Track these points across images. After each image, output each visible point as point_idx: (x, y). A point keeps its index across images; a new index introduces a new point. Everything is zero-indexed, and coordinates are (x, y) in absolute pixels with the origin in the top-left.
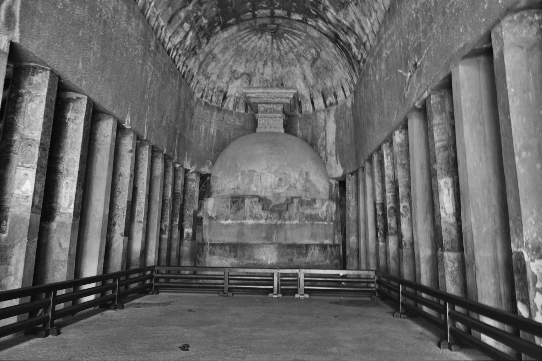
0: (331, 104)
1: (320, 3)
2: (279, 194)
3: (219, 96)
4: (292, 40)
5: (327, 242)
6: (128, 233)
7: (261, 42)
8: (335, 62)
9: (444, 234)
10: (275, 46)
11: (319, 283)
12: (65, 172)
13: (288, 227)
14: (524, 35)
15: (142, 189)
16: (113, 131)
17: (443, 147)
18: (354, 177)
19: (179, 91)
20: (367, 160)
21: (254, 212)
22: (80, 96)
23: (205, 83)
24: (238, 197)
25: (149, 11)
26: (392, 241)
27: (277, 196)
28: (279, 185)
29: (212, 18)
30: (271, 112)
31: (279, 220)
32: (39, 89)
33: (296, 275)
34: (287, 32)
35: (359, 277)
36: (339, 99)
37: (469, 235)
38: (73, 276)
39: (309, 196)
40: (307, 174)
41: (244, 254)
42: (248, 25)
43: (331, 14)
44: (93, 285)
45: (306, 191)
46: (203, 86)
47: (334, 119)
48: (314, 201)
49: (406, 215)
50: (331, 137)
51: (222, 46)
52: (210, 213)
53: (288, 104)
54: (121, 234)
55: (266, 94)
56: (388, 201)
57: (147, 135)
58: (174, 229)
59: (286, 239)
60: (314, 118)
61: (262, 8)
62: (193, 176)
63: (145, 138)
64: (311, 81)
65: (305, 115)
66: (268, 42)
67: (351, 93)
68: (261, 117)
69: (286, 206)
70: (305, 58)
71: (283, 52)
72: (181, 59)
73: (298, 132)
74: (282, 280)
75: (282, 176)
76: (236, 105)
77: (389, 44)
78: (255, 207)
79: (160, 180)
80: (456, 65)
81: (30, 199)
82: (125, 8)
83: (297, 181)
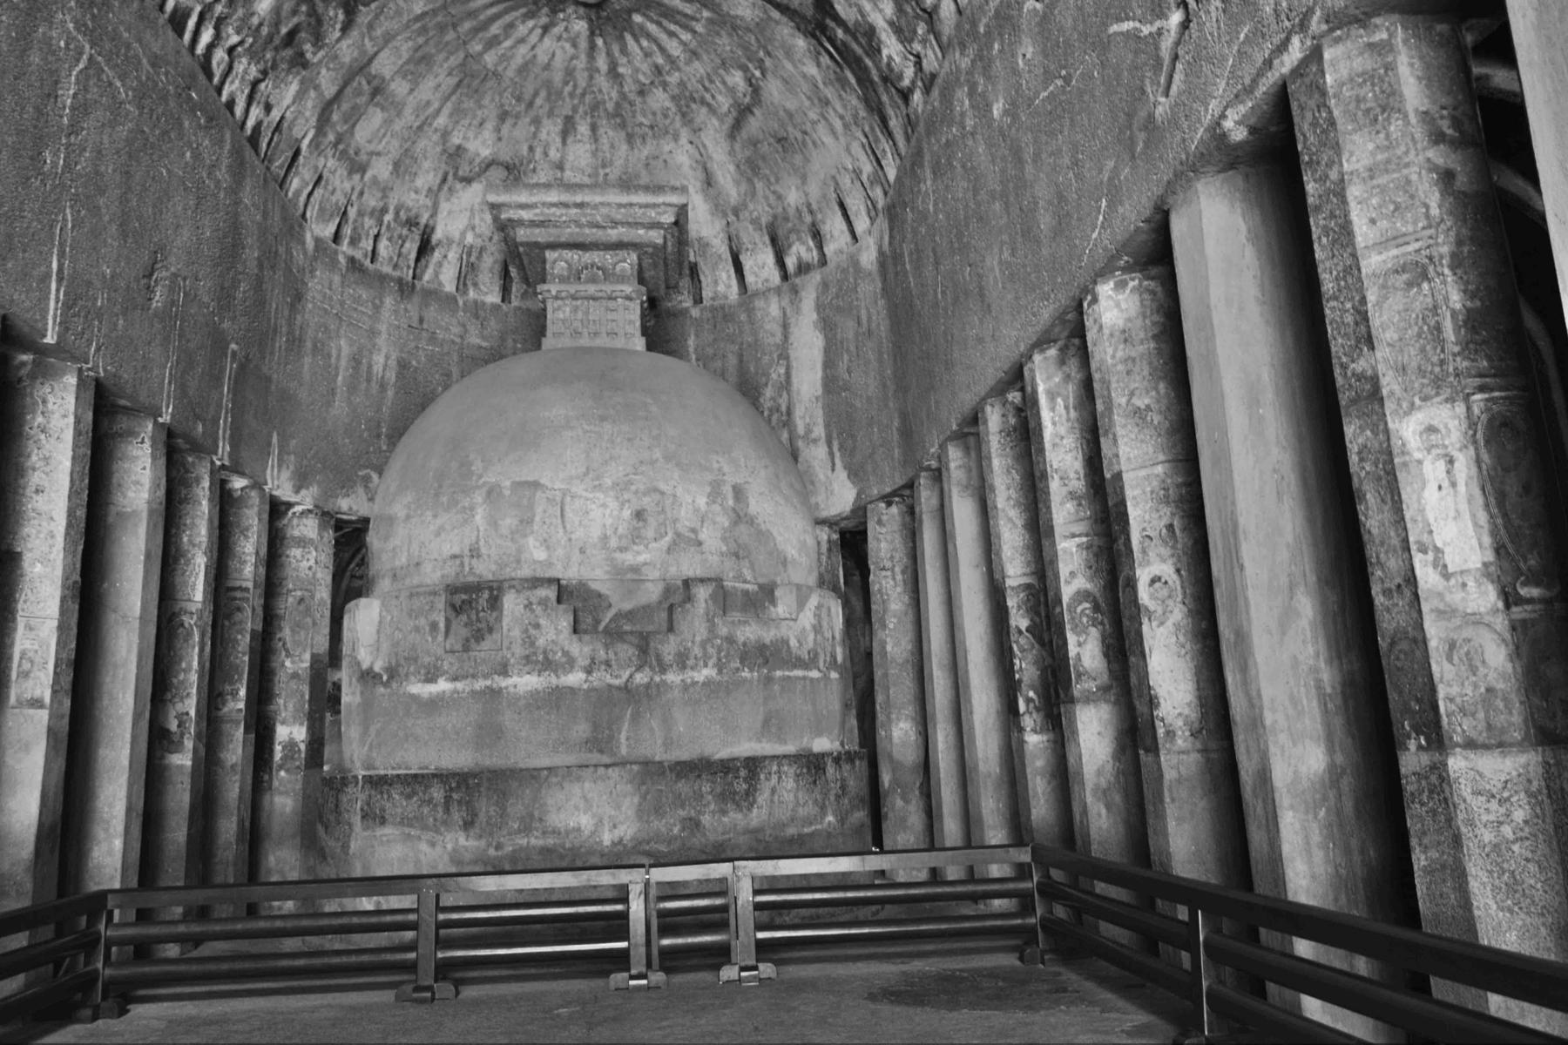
0: (803, 268)
2: (635, 569)
4: (663, 37)
10: (602, 63)
15: (45, 561)
18: (894, 510)
20: (950, 439)
21: (541, 642)
23: (347, 186)
24: (477, 588)
27: (630, 577)
28: (636, 537)
30: (593, 280)
31: (639, 668)
33: (721, 888)
36: (829, 249)
39: (748, 575)
40: (738, 492)
41: (503, 814)
45: (737, 555)
47: (815, 316)
48: (768, 592)
50: (808, 380)
51: (405, 47)
52: (365, 657)
53: (655, 246)
55: (574, 211)
57: (65, 326)
59: (668, 744)
60: (743, 317)
63: (50, 339)
64: (732, 190)
65: (713, 309)
66: (575, 45)
68: (556, 298)
69: (664, 615)
70: (709, 105)
71: (629, 87)
72: (240, 67)
74: (663, 914)
75: (647, 502)
76: (465, 278)
78: (542, 622)
79: (142, 530)
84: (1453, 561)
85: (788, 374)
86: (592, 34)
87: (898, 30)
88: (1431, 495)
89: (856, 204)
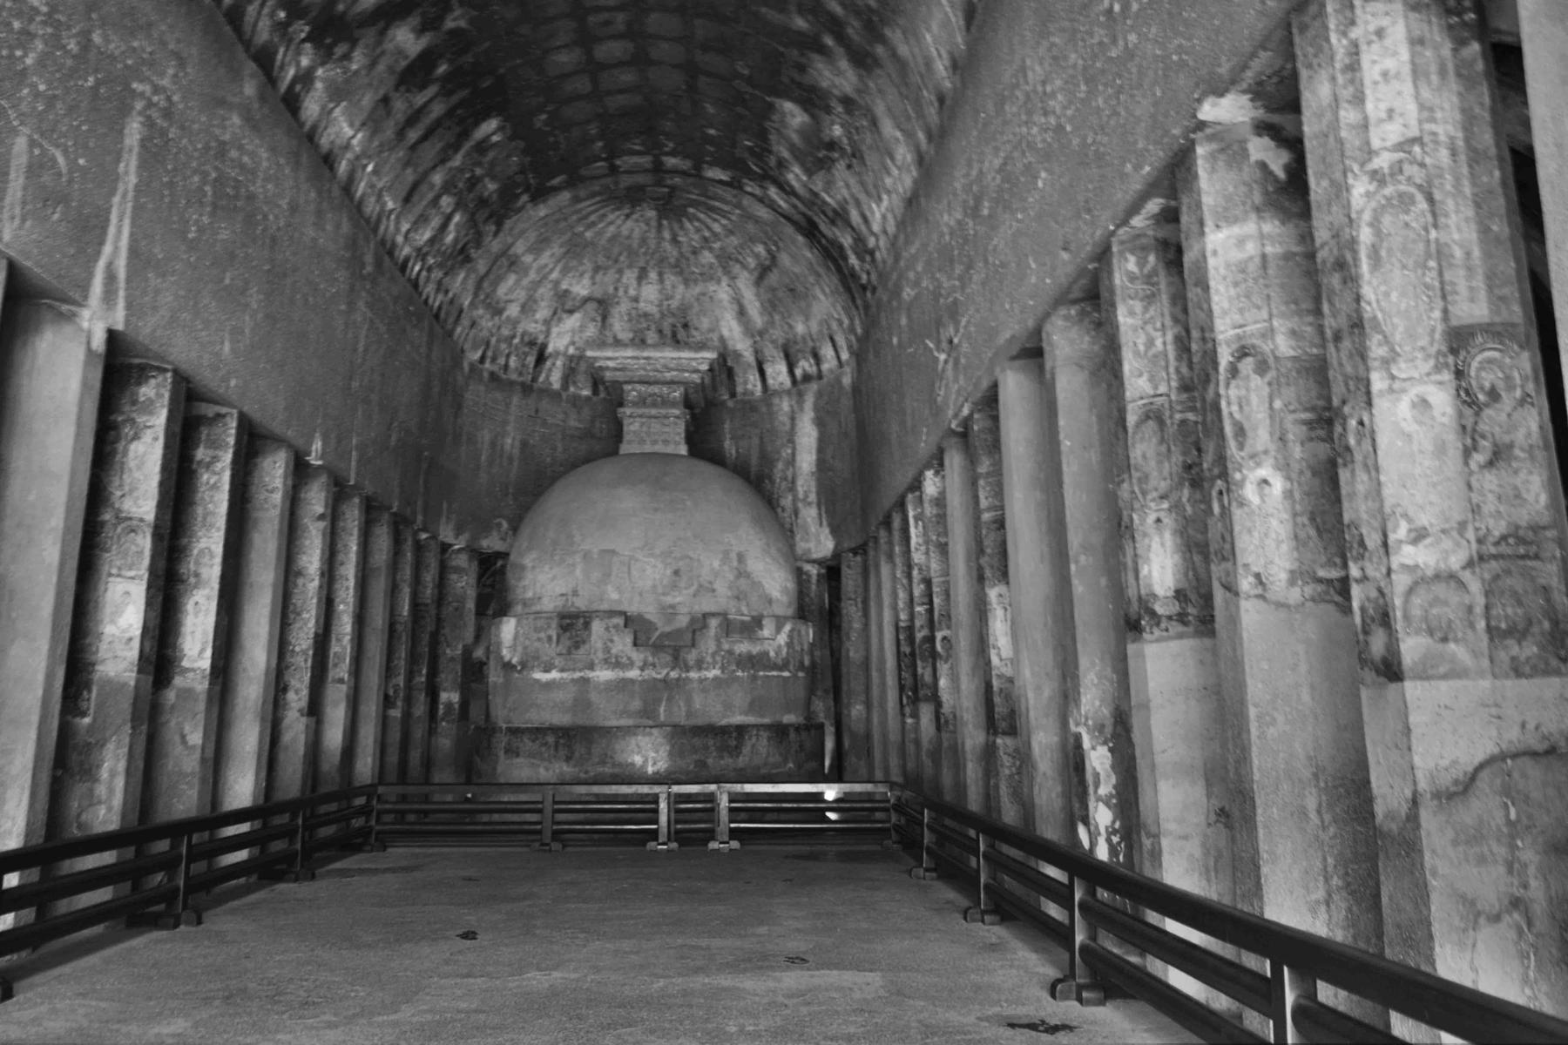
0: (807, 378)
1: (770, 152)
2: (672, 607)
3: (526, 354)
4: (708, 221)
5: (789, 718)
6: (315, 709)
7: (631, 226)
8: (811, 279)
10: (667, 235)
11: (769, 816)
12: (192, 580)
13: (695, 685)
14: (1085, 346)
15: (346, 604)
16: (285, 477)
18: (859, 558)
19: (428, 356)
21: (614, 651)
22: (224, 410)
24: (576, 616)
25: (363, 184)
26: (926, 712)
27: (670, 612)
29: (509, 178)
30: (654, 405)
32: (151, 413)
33: (710, 798)
34: (694, 204)
35: (869, 797)
36: (825, 367)
38: (208, 807)
39: (745, 610)
40: (741, 558)
41: (589, 753)
42: (597, 188)
43: (795, 176)
44: (244, 828)
45: (738, 598)
46: (485, 333)
48: (758, 622)
50: (807, 460)
51: (532, 236)
52: (506, 653)
54: (300, 710)
56: (918, 623)
57: (357, 474)
58: (415, 693)
59: (689, 714)
62: (462, 560)
64: (758, 320)
65: (744, 402)
73: (727, 444)
74: (678, 811)
76: (567, 378)
80: (1003, 370)
81: (136, 644)
82: (313, 195)
83: (716, 574)
84: (1004, 655)
85: (794, 454)
86: (660, 218)
87: (856, 254)
89: (841, 340)
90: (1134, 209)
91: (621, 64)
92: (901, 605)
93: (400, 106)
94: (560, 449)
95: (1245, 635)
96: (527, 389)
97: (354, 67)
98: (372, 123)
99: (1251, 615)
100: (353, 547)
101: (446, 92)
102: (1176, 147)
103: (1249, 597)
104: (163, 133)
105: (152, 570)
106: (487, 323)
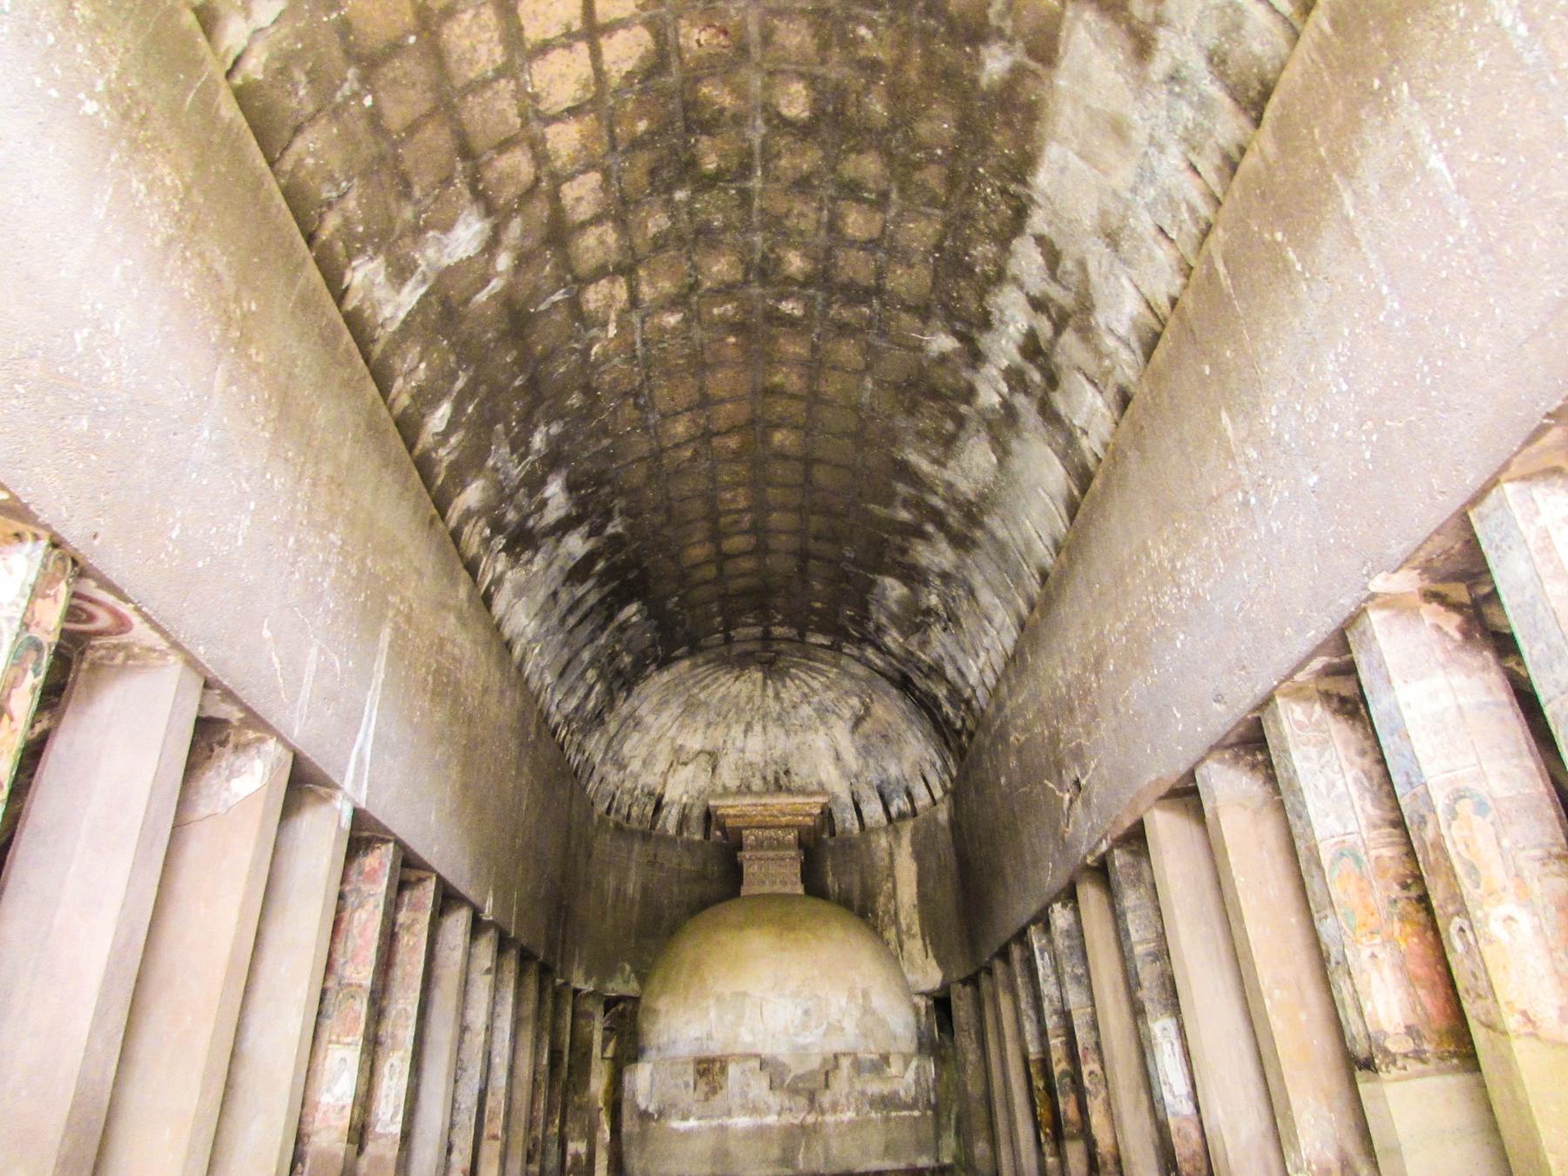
0: (902, 816)
2: (804, 1047)
4: (809, 680)
7: (743, 686)
8: (904, 726)
9: (1175, 1140)
10: (770, 692)
12: (389, 1041)
17: (1148, 954)
18: (968, 989)
21: (751, 1096)
22: (422, 874)
24: (712, 1061)
26: (1075, 1153)
27: (802, 1052)
30: (771, 847)
32: (374, 882)
34: (797, 665)
36: (919, 804)
37: (1218, 1144)
40: (865, 995)
42: (713, 656)
43: (893, 639)
45: (865, 1036)
46: (612, 788)
48: (885, 1059)
49: (1098, 1092)
51: (655, 699)
52: (642, 1103)
61: (746, 625)
66: (754, 684)
67: (946, 792)
73: (830, 880)
75: (810, 1004)
76: (683, 822)
77: (1020, 722)
82: (498, 676)
85: (895, 888)
86: (765, 678)
88: (1166, 1058)
90: (1301, 665)
91: (742, 554)
92: (1028, 1037)
93: (564, 598)
94: (676, 890)
95: (1524, 1076)
96: (646, 836)
97: (535, 569)
98: (544, 613)
99: (1524, 1054)
100: (510, 999)
101: (601, 584)
102: (1346, 614)
103: (1518, 1036)
104: (404, 634)
105: (366, 1038)
106: (613, 777)
